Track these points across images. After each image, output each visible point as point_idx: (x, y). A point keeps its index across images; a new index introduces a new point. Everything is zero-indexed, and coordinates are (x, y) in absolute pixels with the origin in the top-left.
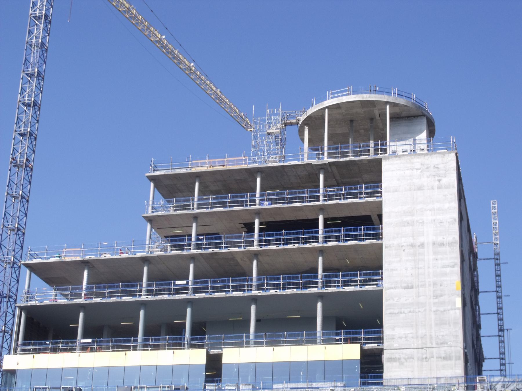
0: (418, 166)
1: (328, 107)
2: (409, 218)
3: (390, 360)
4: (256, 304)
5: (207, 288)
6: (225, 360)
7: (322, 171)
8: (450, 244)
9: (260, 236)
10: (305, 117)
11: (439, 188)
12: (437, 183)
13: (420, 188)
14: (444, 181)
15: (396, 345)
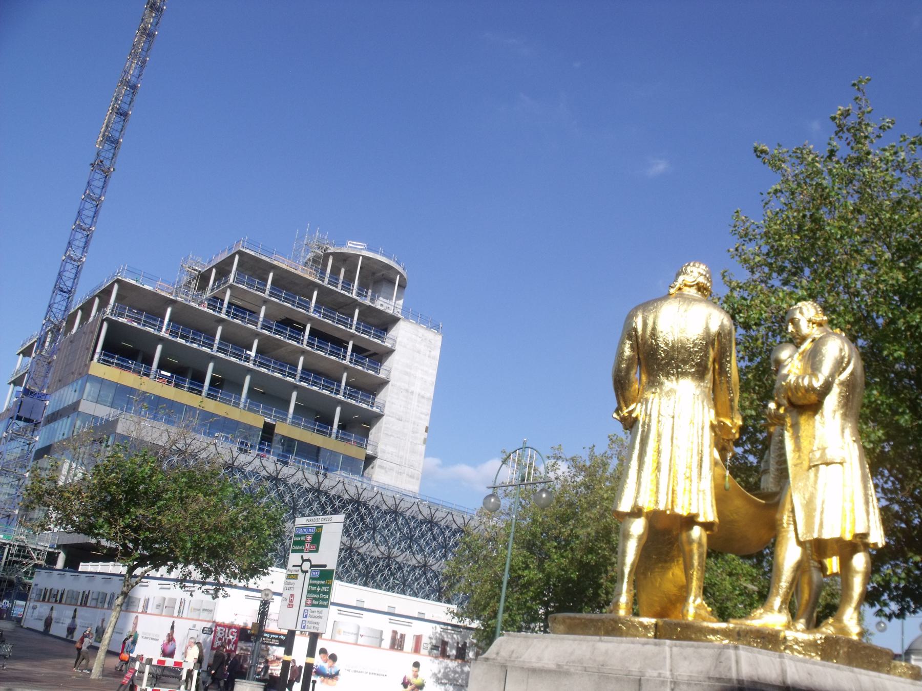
0: (420, 335)
1: (363, 256)
2: (408, 370)
3: (381, 467)
4: (297, 391)
5: (270, 366)
6: (276, 431)
7: (317, 289)
8: (428, 399)
9: (352, 355)
10: (339, 251)
11: (429, 357)
12: (428, 353)
13: (419, 352)
14: (433, 353)
15: (385, 458)
